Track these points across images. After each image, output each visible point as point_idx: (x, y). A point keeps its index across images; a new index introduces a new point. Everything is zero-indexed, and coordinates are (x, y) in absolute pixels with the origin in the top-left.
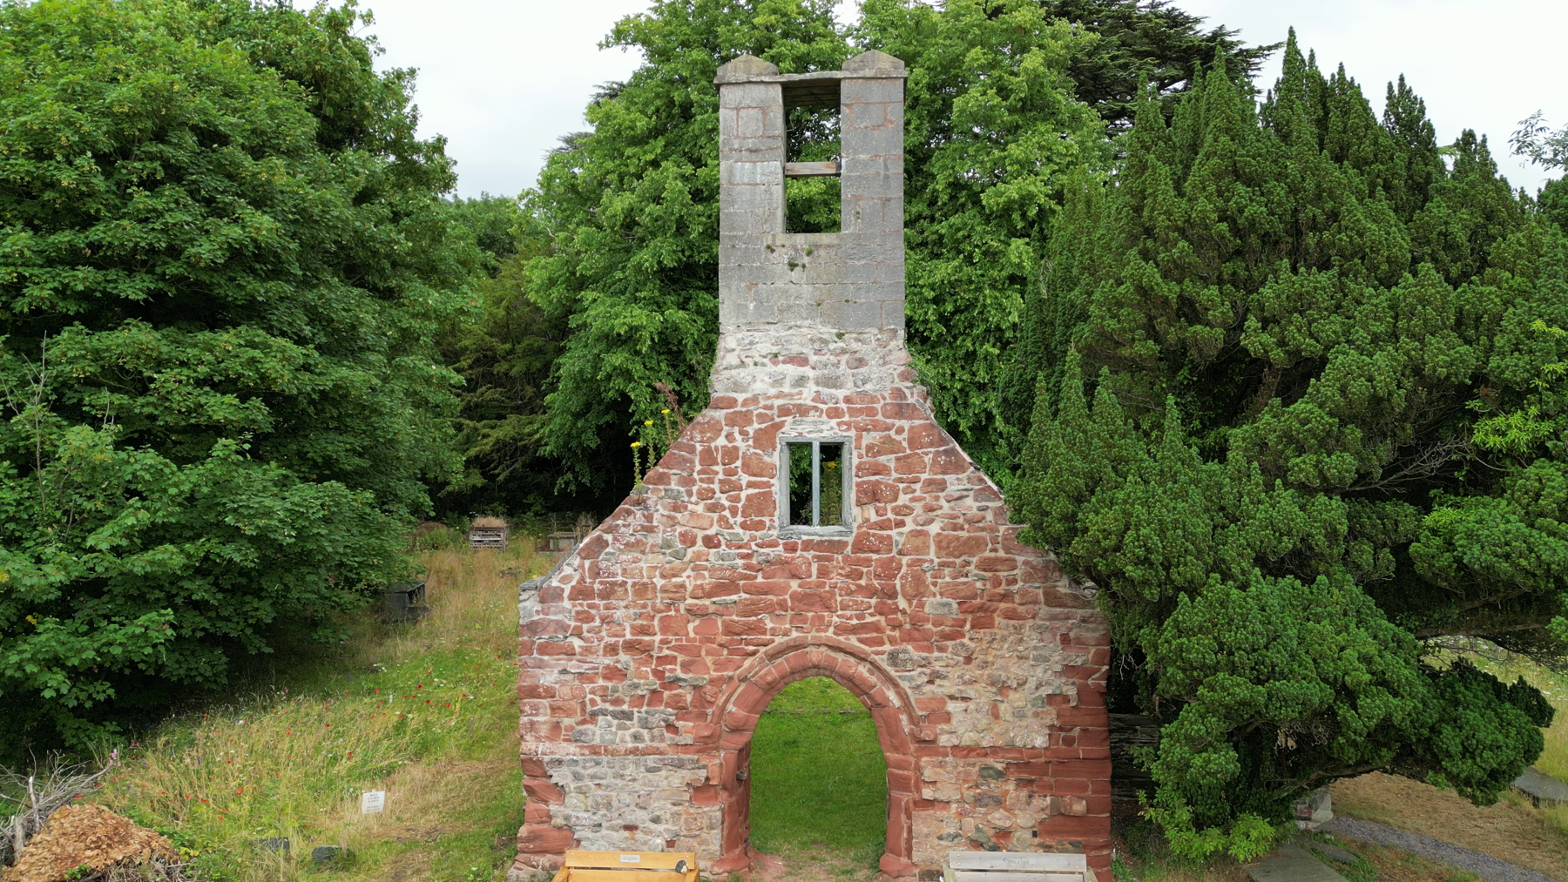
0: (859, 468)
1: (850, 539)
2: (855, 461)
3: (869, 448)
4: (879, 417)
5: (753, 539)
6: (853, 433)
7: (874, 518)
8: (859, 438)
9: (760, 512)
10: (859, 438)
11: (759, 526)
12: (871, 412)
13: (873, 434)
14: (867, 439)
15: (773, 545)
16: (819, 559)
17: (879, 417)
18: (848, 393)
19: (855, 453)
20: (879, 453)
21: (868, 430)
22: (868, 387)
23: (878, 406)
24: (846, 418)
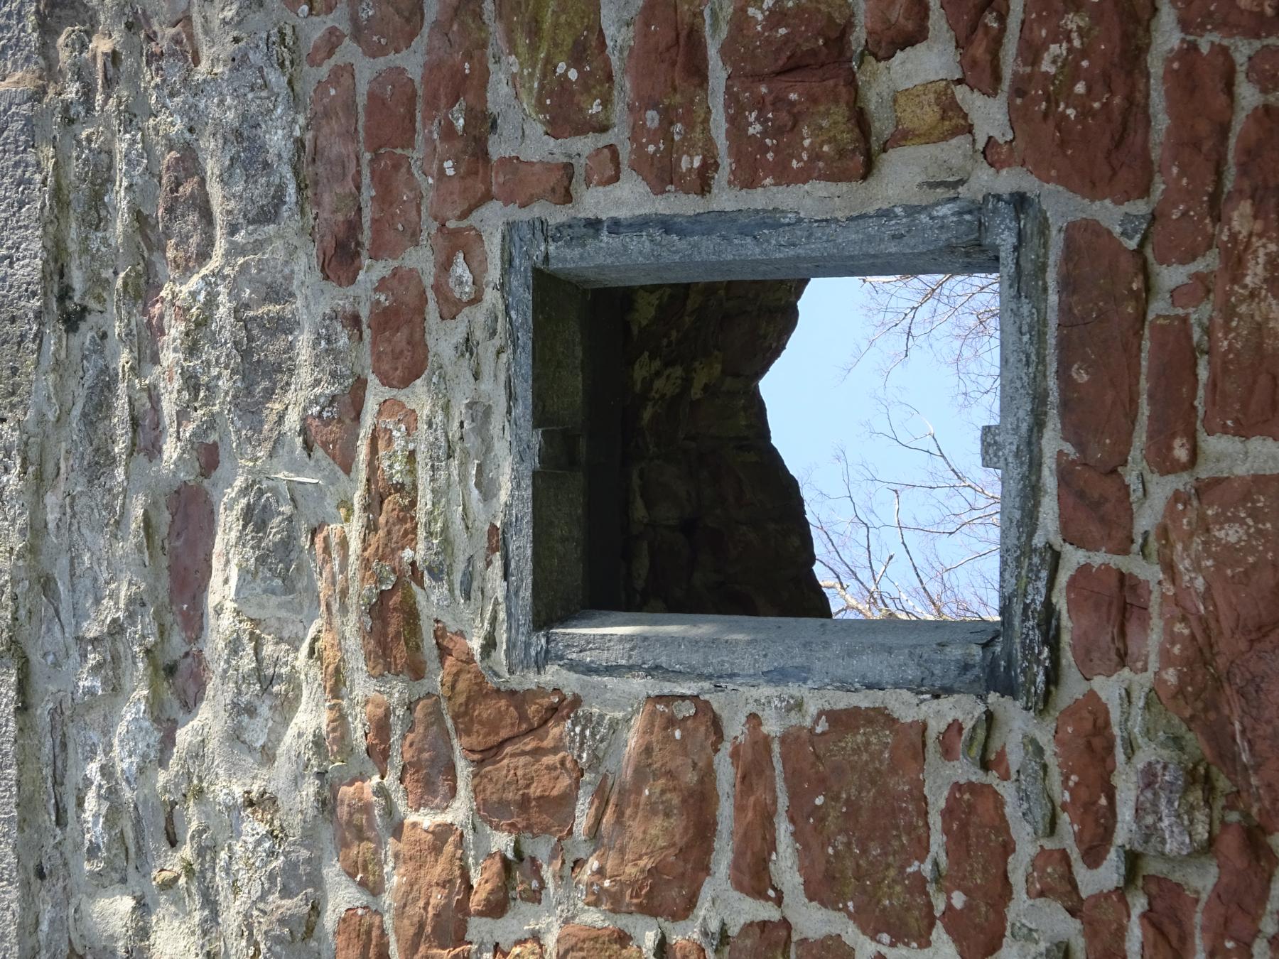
0: (662, 175)
1: (1061, 206)
2: (629, 197)
3: (563, 115)
4: (412, 61)
5: (1058, 885)
6: (492, 221)
7: (930, 62)
8: (518, 182)
9: (895, 820)
10: (518, 182)
11: (976, 823)
12: (391, 118)
13: (499, 92)
14: (524, 139)
15: (1094, 746)
16: (1177, 420)
17: (412, 61)
18: (304, 268)
19: (595, 202)
20: (588, 47)
21: (483, 123)
22: (277, 140)
23: (366, 70)
24: (421, 260)
